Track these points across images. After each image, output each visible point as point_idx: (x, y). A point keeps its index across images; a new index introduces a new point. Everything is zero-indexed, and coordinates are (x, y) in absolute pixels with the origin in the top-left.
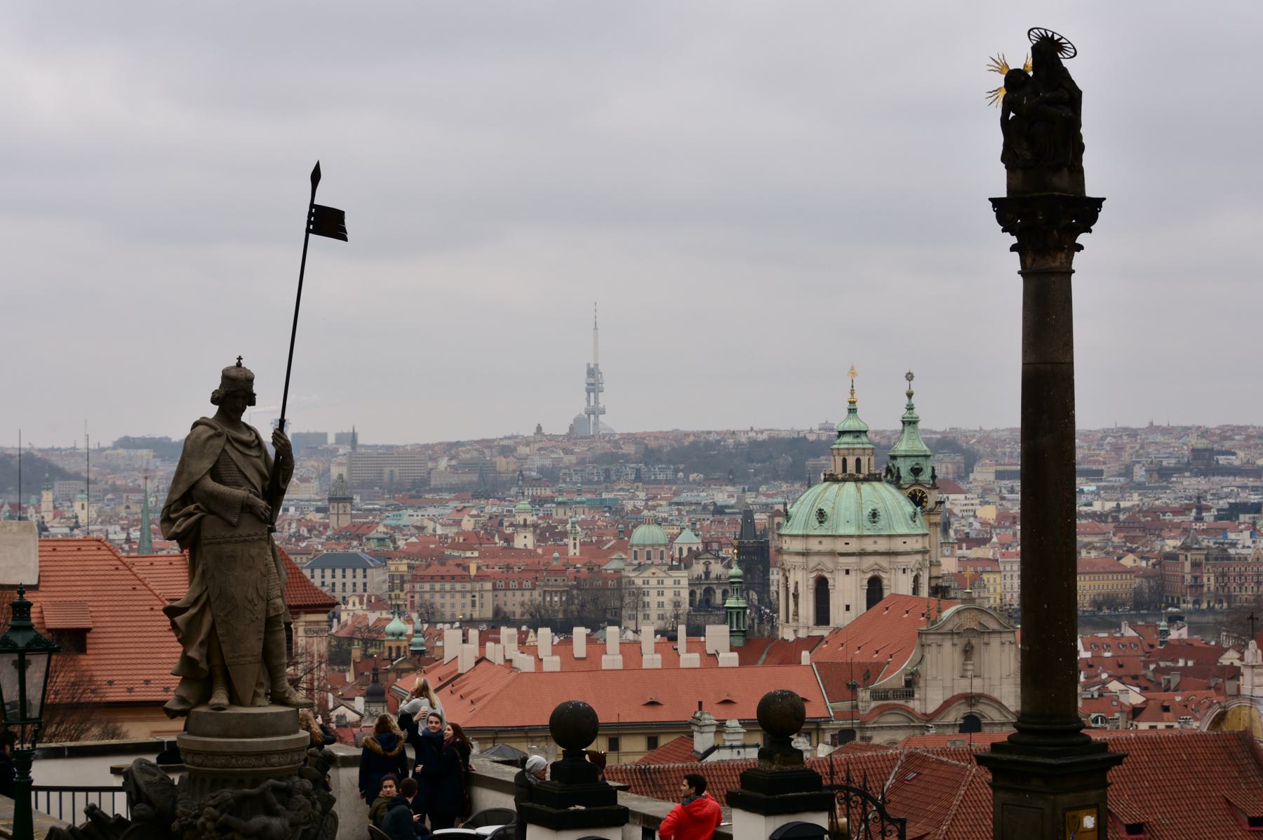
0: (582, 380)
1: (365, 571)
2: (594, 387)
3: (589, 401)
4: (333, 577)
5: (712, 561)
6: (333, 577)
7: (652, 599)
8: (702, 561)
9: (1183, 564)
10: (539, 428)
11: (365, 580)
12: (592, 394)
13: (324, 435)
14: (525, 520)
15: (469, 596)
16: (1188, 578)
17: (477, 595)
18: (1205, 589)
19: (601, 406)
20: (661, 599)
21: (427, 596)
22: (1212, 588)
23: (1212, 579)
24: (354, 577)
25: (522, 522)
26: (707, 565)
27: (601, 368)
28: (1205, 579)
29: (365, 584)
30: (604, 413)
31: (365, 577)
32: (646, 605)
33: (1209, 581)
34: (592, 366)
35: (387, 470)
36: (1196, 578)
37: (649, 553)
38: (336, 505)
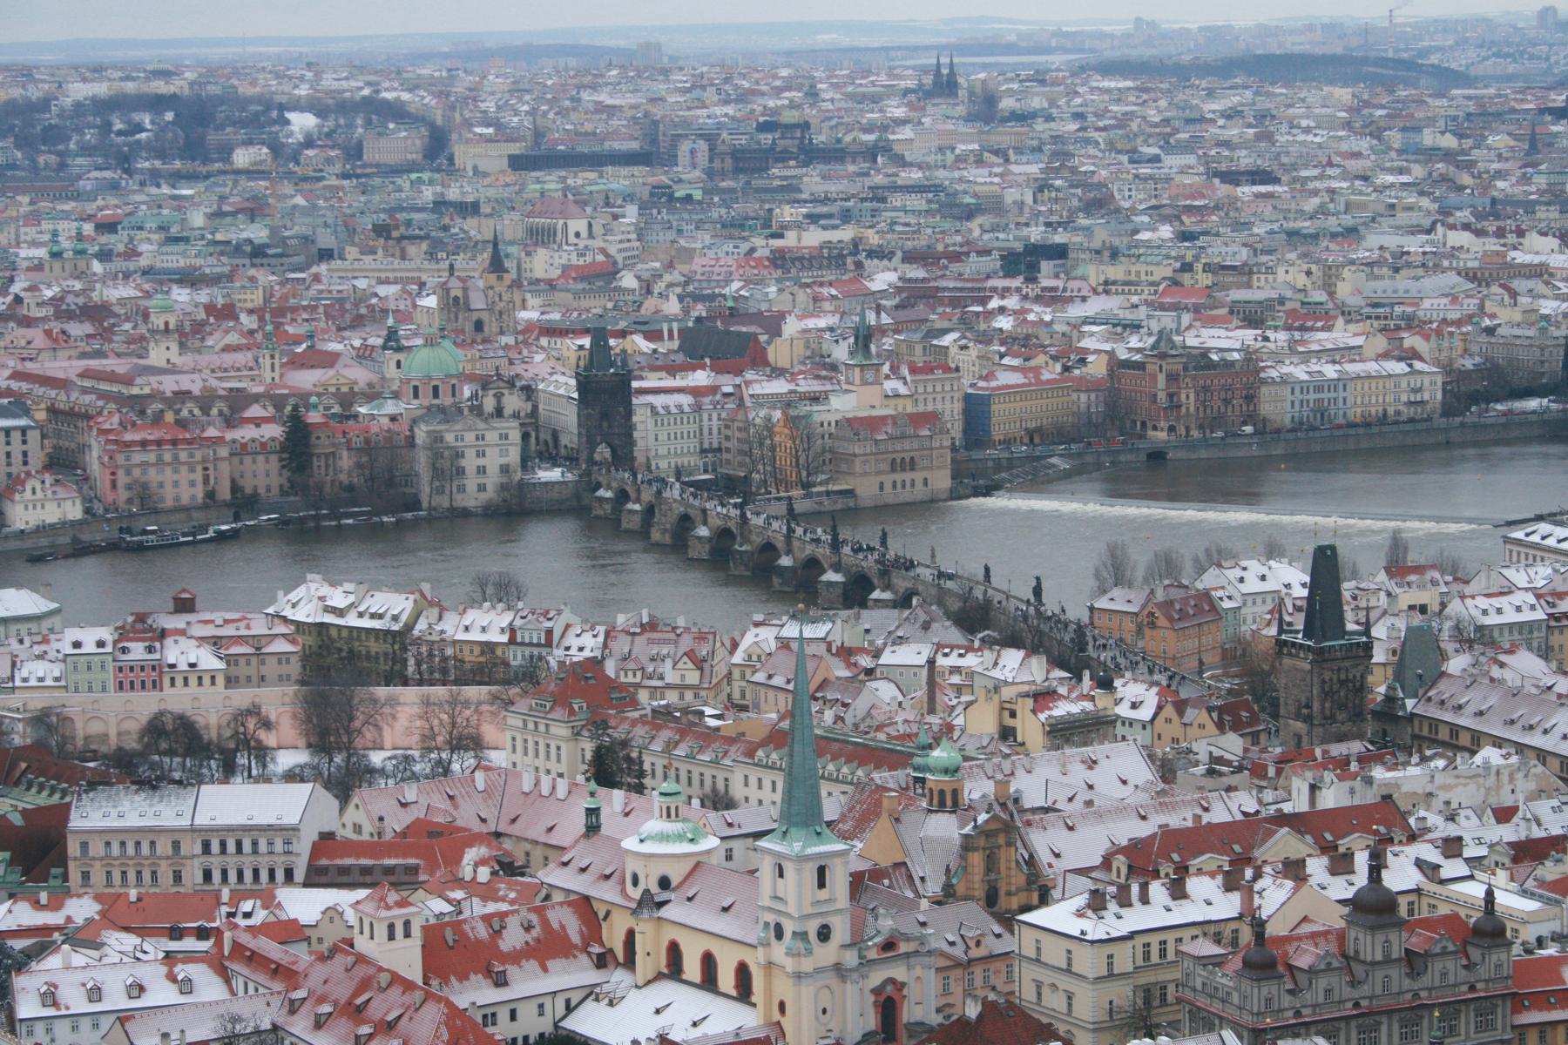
5: (506, 392)
7: (470, 462)
8: (491, 393)
9: (1154, 377)
14: (167, 324)
15: (199, 468)
16: (1162, 396)
17: (211, 466)
18: (1183, 410)
20: (481, 462)
21: (137, 472)
22: (1192, 409)
23: (1192, 396)
25: (162, 327)
26: (498, 397)
28: (1183, 397)
29: (25, 454)
31: (24, 442)
32: (461, 472)
33: (1188, 398)
36: (1171, 396)
37: (436, 389)
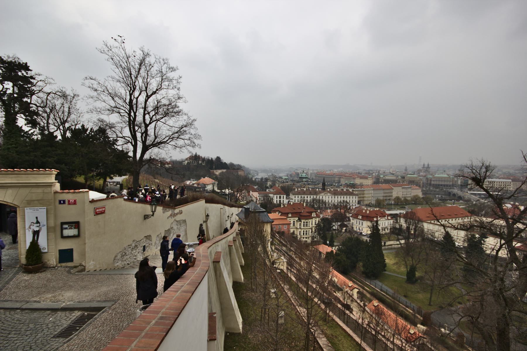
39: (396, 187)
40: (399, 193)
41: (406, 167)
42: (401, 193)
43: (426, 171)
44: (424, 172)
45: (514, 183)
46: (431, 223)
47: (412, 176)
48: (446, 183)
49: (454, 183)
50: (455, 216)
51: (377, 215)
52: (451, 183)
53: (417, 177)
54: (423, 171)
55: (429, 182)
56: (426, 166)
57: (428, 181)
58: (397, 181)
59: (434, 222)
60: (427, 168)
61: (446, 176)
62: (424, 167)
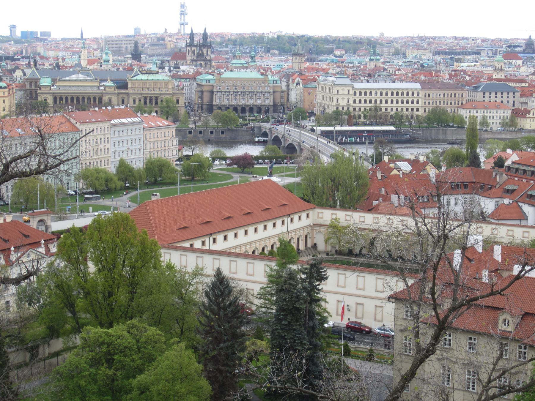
0: (179, 9)
1: (514, 94)
2: (183, 13)
3: (181, 19)
4: (496, 97)
6: (496, 97)
10: (166, 30)
11: (514, 100)
12: (182, 16)
13: (36, 33)
19: (186, 21)
24: (508, 97)
25: (500, 68)
27: (186, 4)
29: (514, 102)
30: (187, 24)
31: (514, 97)
34: (183, 4)
35: (125, 46)
38: (298, 58)
39: (91, 122)
40: (101, 146)
41: (136, 44)
42: (108, 145)
43: (200, 56)
44: (192, 61)
45: (428, 92)
46: (192, 249)
47: (151, 77)
48: (255, 101)
49: (278, 100)
50: (247, 217)
51: (6, 241)
52: (270, 102)
53: (166, 83)
54: (189, 58)
55: (206, 100)
56: (198, 40)
57: (201, 97)
58: (100, 99)
59: (203, 243)
60: (201, 46)
61: (254, 74)
62: (191, 45)
